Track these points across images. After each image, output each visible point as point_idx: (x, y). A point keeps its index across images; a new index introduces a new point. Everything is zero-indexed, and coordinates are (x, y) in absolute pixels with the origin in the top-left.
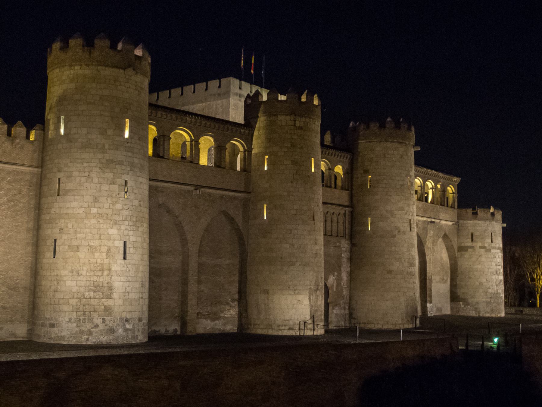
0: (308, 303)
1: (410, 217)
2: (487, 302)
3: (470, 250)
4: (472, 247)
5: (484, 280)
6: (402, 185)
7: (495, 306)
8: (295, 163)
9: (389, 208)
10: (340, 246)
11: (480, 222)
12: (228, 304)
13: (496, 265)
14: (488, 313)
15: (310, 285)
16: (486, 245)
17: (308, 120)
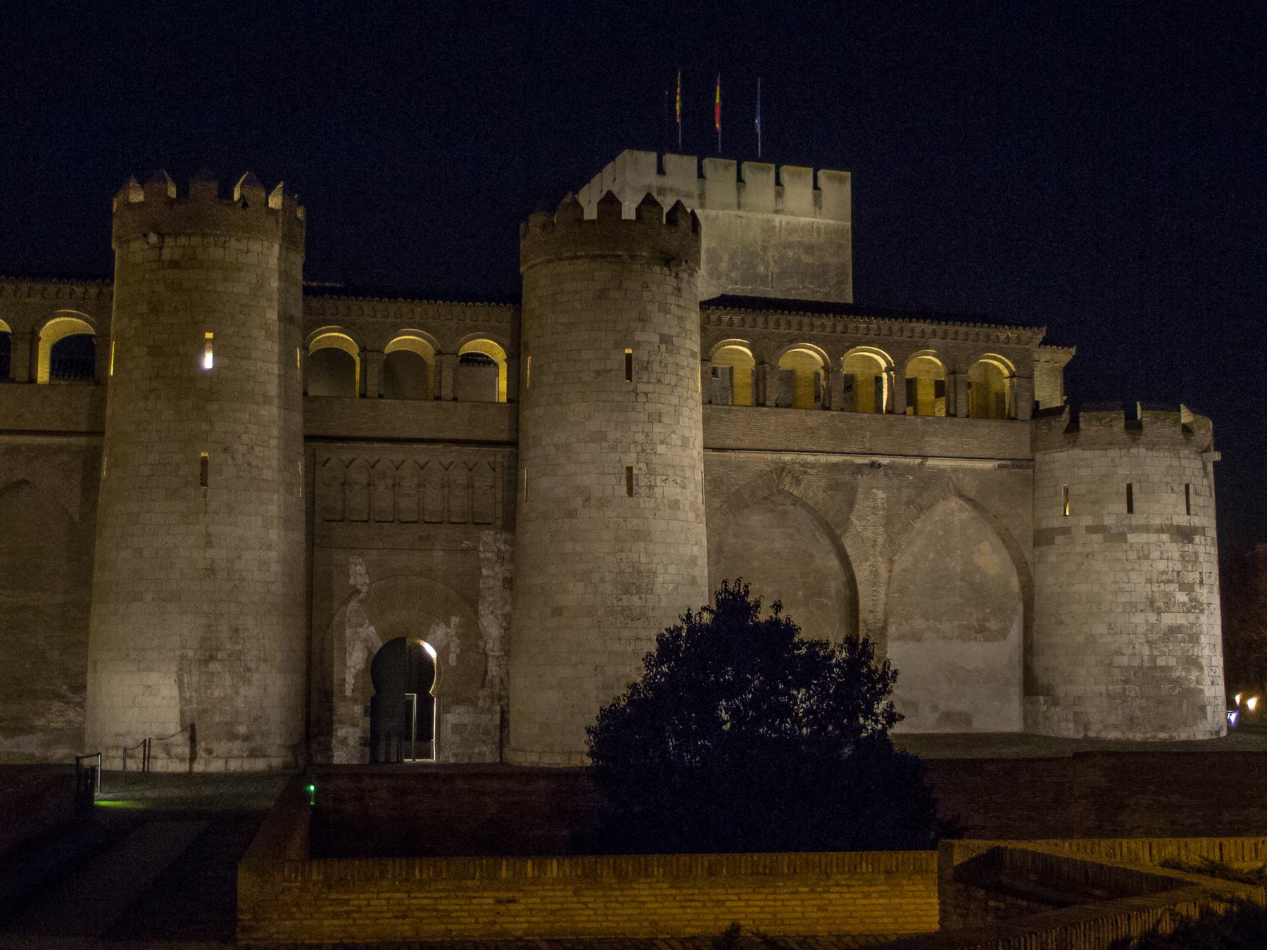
0: (176, 693)
1: (630, 459)
2: (1111, 696)
3: (1059, 539)
4: (1066, 531)
5: (1100, 629)
6: (598, 373)
7: (1141, 709)
10: (475, 549)
11: (1088, 454)
12: (60, 697)
13: (1149, 581)
14: (1116, 727)
16: (1109, 521)
17: (196, 240)
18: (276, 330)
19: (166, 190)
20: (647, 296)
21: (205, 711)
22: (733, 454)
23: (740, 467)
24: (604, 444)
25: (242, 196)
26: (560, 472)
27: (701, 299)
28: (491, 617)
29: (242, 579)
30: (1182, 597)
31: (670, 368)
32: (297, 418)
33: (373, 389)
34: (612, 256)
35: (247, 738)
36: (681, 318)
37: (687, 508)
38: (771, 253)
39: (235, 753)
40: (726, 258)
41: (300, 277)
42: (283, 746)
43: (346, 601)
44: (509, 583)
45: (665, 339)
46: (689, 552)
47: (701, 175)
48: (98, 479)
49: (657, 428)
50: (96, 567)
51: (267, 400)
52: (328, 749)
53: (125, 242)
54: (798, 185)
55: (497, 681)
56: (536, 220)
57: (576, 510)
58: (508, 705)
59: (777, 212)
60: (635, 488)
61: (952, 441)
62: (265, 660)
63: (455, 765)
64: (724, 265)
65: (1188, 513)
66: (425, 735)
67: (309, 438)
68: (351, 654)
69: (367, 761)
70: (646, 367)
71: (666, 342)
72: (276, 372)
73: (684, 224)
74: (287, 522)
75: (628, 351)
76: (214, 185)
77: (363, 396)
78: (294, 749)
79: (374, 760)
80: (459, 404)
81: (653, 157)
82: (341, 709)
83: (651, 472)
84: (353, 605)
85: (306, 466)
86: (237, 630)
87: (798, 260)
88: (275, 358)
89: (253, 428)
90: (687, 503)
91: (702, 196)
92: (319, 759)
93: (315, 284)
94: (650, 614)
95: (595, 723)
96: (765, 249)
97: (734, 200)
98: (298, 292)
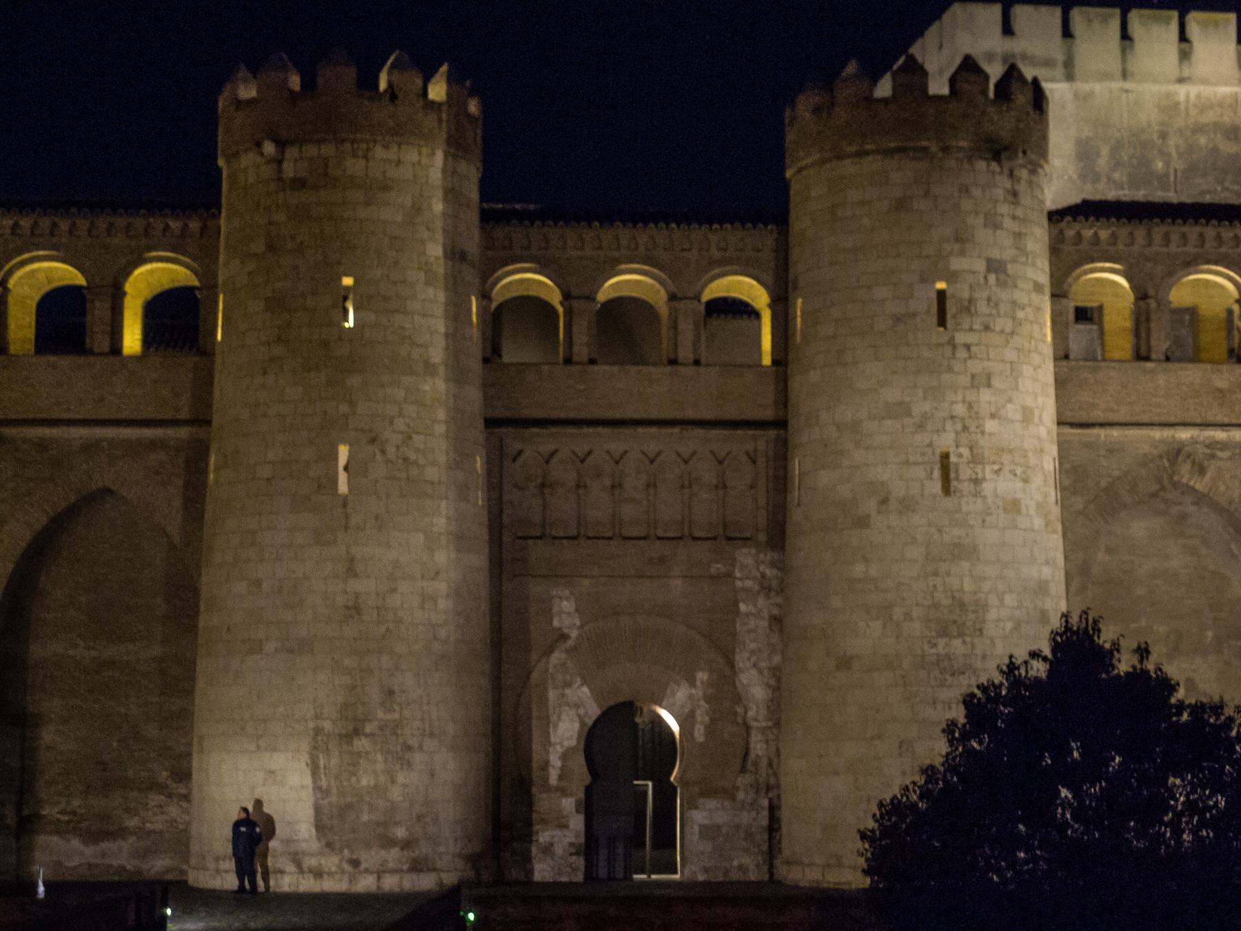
0: (308, 780)
1: (946, 441)
6: (898, 319)
8: (276, 304)
9: (846, 413)
10: (729, 575)
15: (317, 717)
17: (328, 150)
18: (441, 271)
19: (285, 80)
20: (966, 204)
21: (349, 806)
22: (1102, 433)
23: (1113, 450)
24: (907, 421)
25: (390, 85)
26: (846, 463)
27: (1050, 205)
28: (753, 672)
29: (399, 621)
31: (1003, 308)
32: (474, 394)
33: (581, 351)
34: (915, 149)
35: (407, 845)
36: (1018, 236)
37: (1032, 511)
38: (1172, 142)
39: (391, 865)
40: (1105, 151)
41: (475, 196)
42: (460, 855)
43: (549, 650)
44: (777, 622)
45: (995, 266)
46: (1035, 574)
47: (1067, 33)
48: (204, 484)
49: (985, 396)
50: (202, 608)
51: (430, 369)
52: (527, 859)
53: (233, 156)
55: (764, 762)
56: (804, 106)
57: (868, 516)
58: (779, 796)
59: (1181, 80)
60: (954, 483)
62: (432, 735)
63: (706, 884)
64: (1103, 162)
66: (665, 840)
67: (491, 423)
68: (556, 726)
69: (579, 877)
70: (968, 307)
71: (996, 272)
72: (442, 329)
73: (1022, 99)
74: (460, 540)
75: (941, 285)
76: (350, 75)
77: (568, 361)
78: (473, 860)
79: (590, 876)
80: (702, 370)
81: (996, 10)
82: (543, 803)
83: (977, 459)
84: (557, 657)
85: (489, 461)
86: (391, 693)
87: (1215, 151)
88: (439, 310)
89: (411, 410)
90: (1032, 504)
91: (1069, 64)
92: (515, 874)
93: (500, 206)
94: (979, 665)
95: (871, 824)
96: (1163, 136)
97: (1115, 65)
98: (472, 216)
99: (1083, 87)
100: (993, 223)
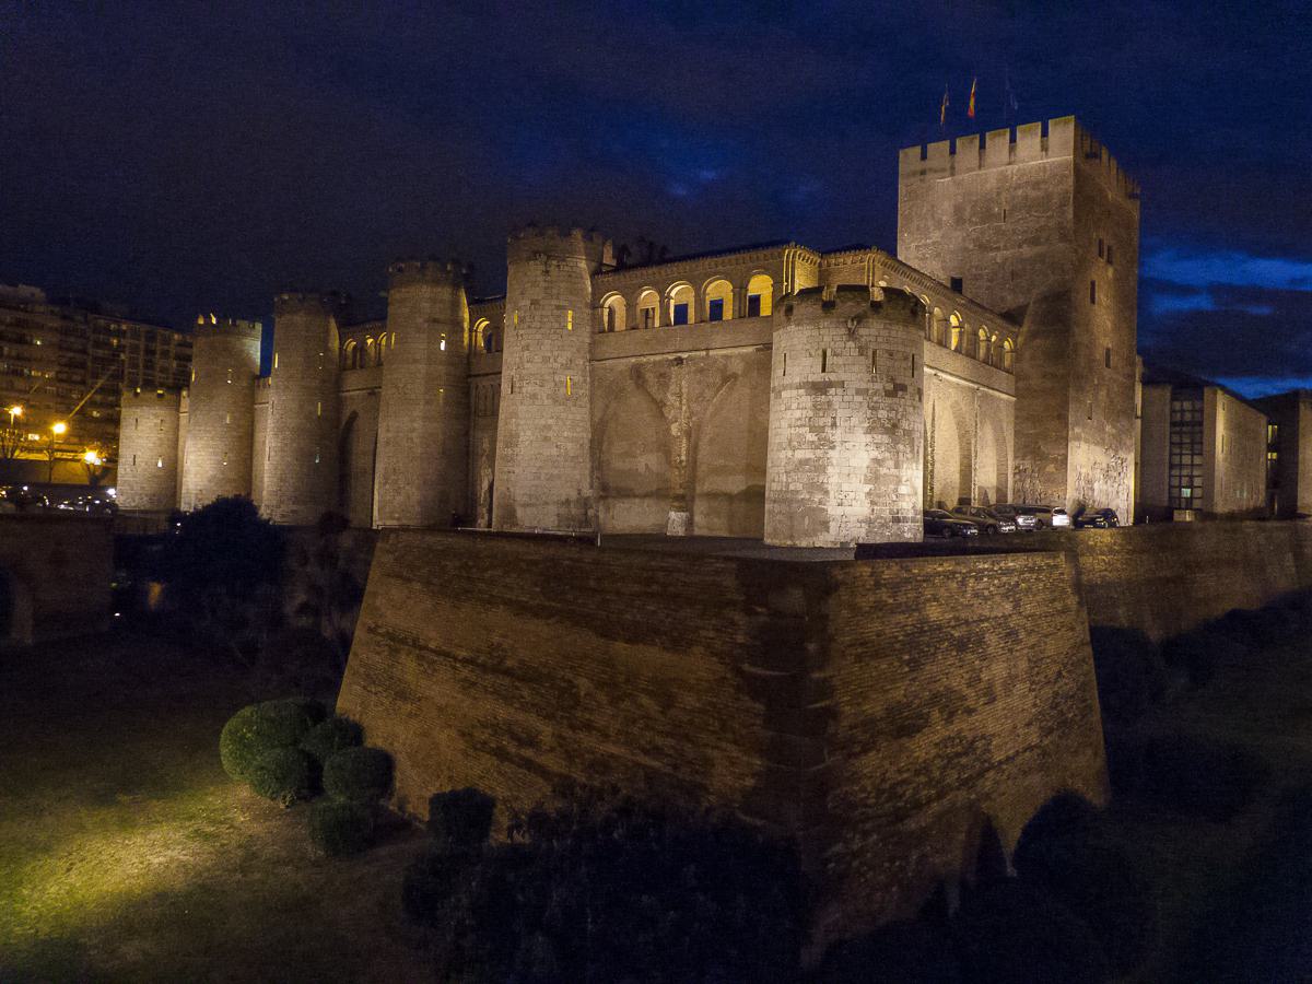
22: (607, 362)
30: (811, 437)
35: (398, 519)
40: (968, 210)
47: (953, 151)
49: (526, 353)
54: (1029, 139)
59: (1010, 164)
61: (729, 337)
64: (967, 214)
65: (824, 370)
84: (484, 458)
91: (953, 168)
96: (998, 194)
97: (976, 162)
99: (958, 177)
100: (534, 284)
